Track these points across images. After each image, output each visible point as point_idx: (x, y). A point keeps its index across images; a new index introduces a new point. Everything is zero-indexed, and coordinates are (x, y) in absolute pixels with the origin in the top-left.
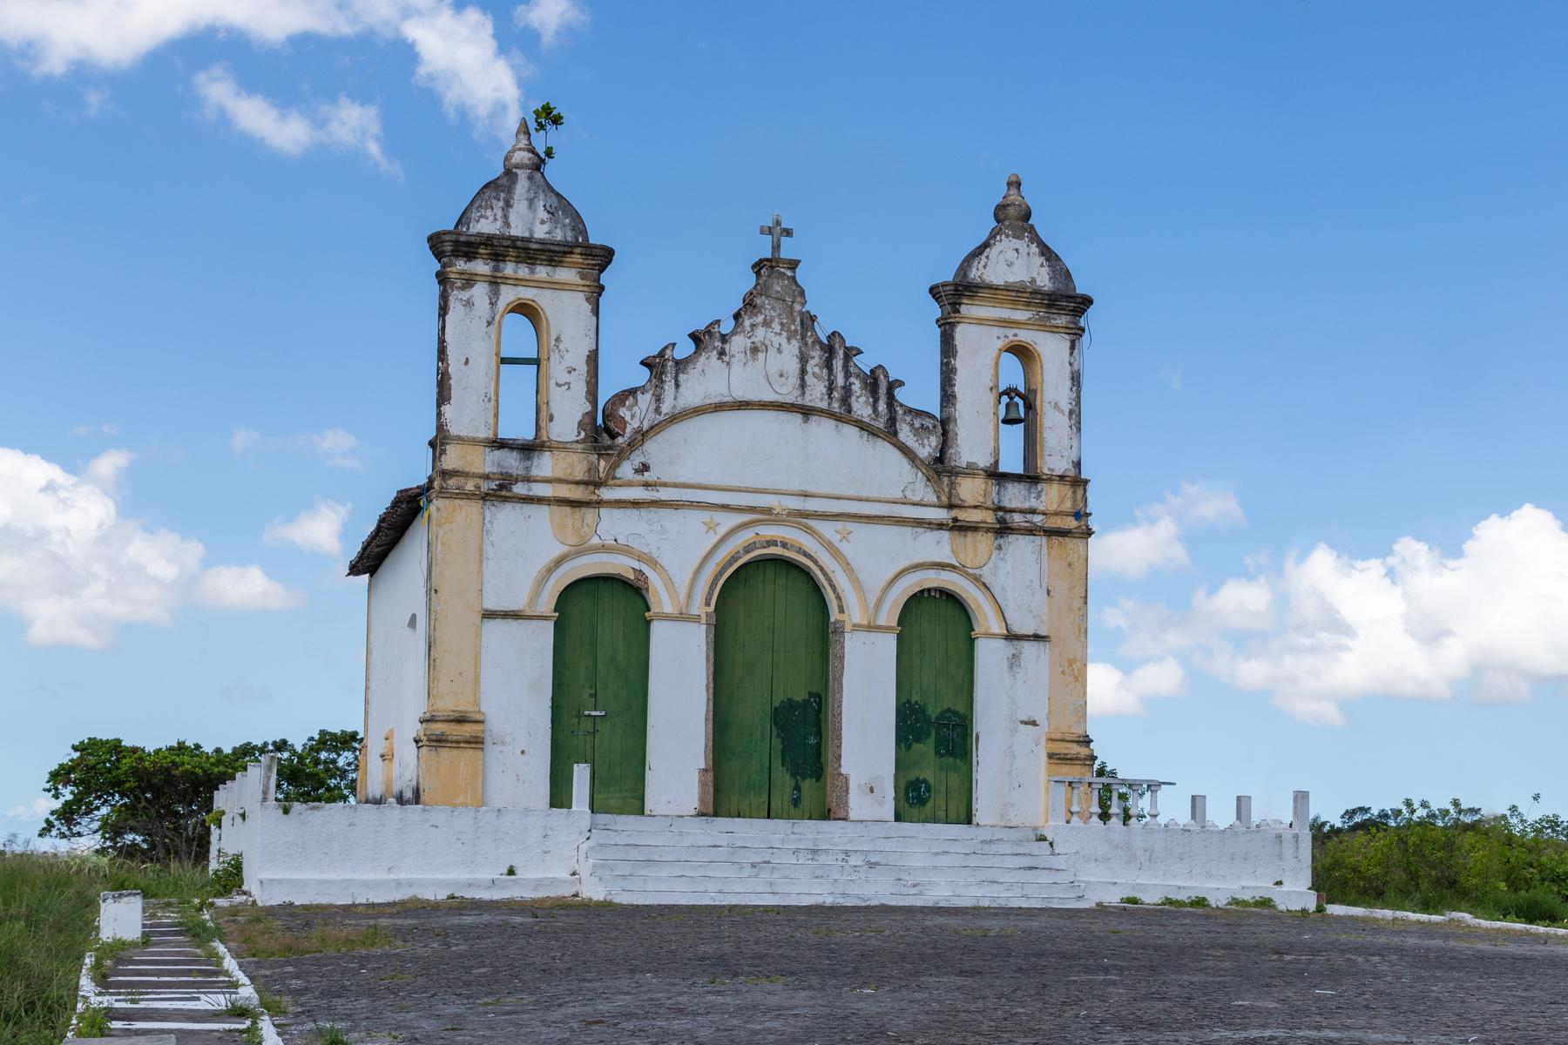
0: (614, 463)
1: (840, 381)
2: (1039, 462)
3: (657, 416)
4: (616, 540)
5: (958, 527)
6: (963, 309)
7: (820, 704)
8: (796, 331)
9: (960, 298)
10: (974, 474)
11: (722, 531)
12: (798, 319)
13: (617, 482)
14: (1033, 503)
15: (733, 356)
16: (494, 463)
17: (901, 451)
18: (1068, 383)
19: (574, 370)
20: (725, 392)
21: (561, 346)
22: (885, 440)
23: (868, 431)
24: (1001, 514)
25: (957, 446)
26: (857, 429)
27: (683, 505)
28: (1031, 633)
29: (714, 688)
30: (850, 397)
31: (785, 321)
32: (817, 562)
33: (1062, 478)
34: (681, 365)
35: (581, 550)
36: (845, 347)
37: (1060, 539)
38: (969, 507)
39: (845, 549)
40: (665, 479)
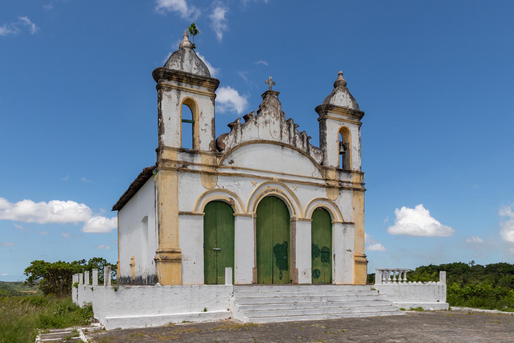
0: (222, 160)
1: (293, 135)
2: (351, 166)
3: (236, 144)
4: (223, 187)
5: (329, 187)
6: (328, 114)
7: (287, 245)
8: (279, 117)
9: (327, 110)
10: (333, 169)
11: (258, 185)
12: (279, 113)
13: (224, 166)
14: (349, 180)
15: (259, 124)
16: (181, 158)
17: (311, 160)
18: (358, 141)
19: (207, 125)
20: (257, 137)
21: (203, 116)
22: (306, 156)
23: (301, 153)
24: (340, 183)
25: (327, 159)
26: (298, 152)
27: (245, 175)
28: (349, 222)
29: (257, 240)
30: (296, 141)
31: (275, 113)
32: (287, 197)
33: (357, 172)
34: (242, 126)
35: (212, 191)
36: (294, 124)
37: (357, 191)
38: (332, 180)
39: (295, 192)
40: (239, 166)
